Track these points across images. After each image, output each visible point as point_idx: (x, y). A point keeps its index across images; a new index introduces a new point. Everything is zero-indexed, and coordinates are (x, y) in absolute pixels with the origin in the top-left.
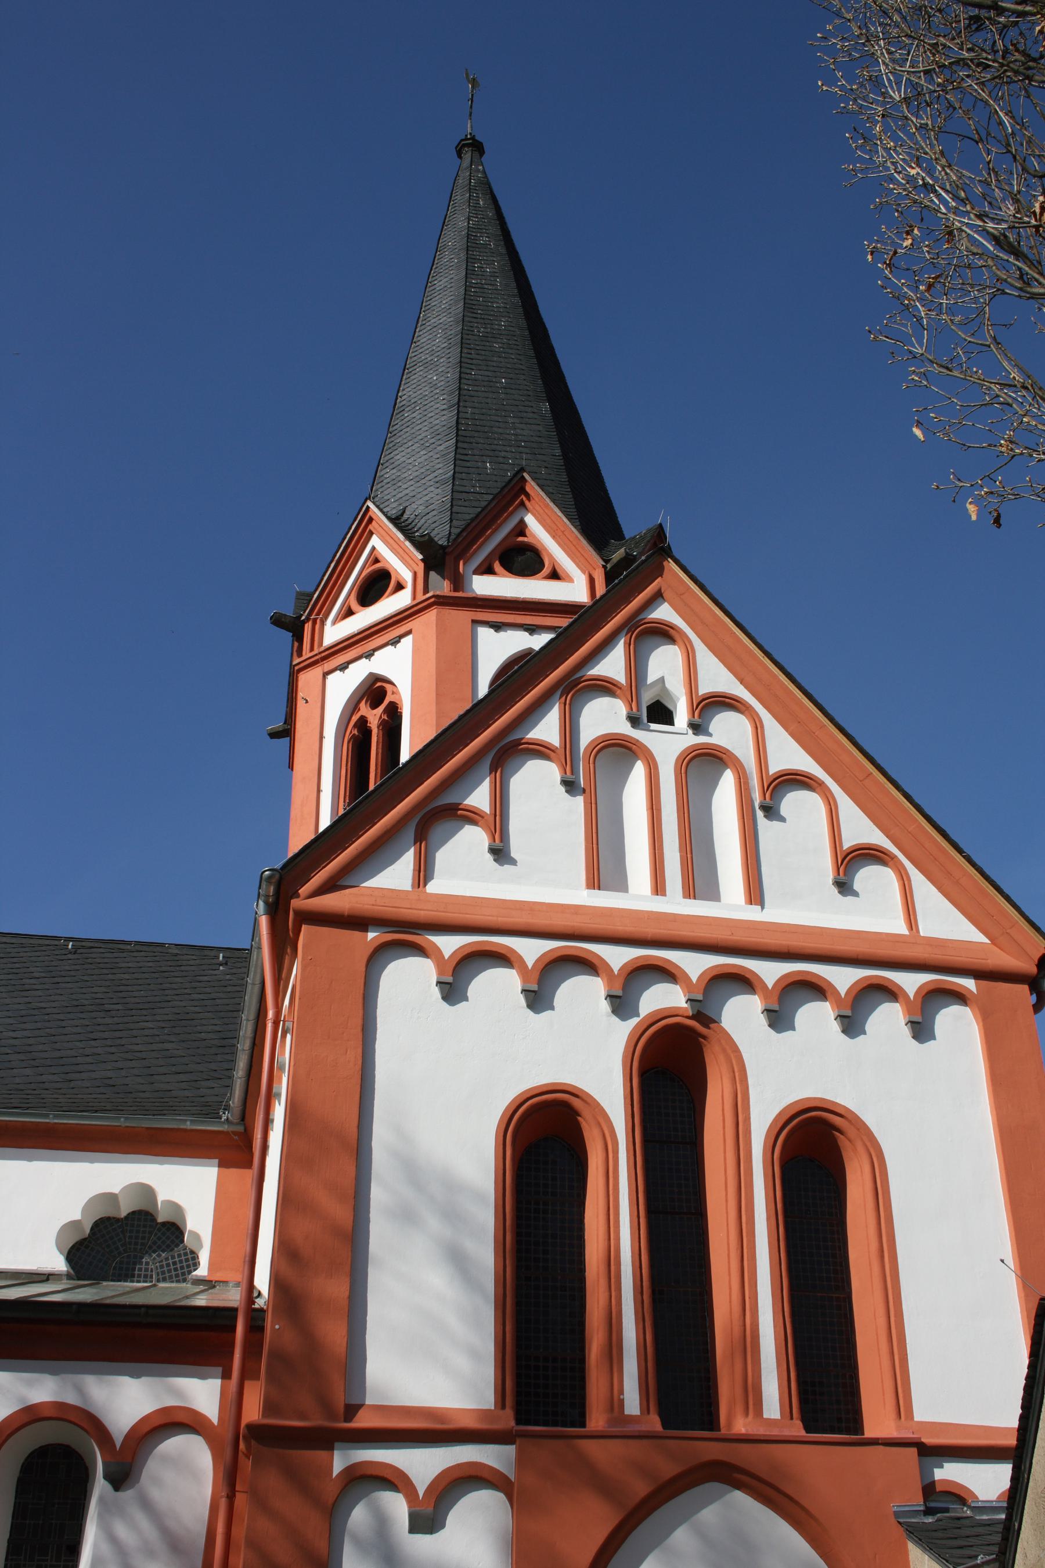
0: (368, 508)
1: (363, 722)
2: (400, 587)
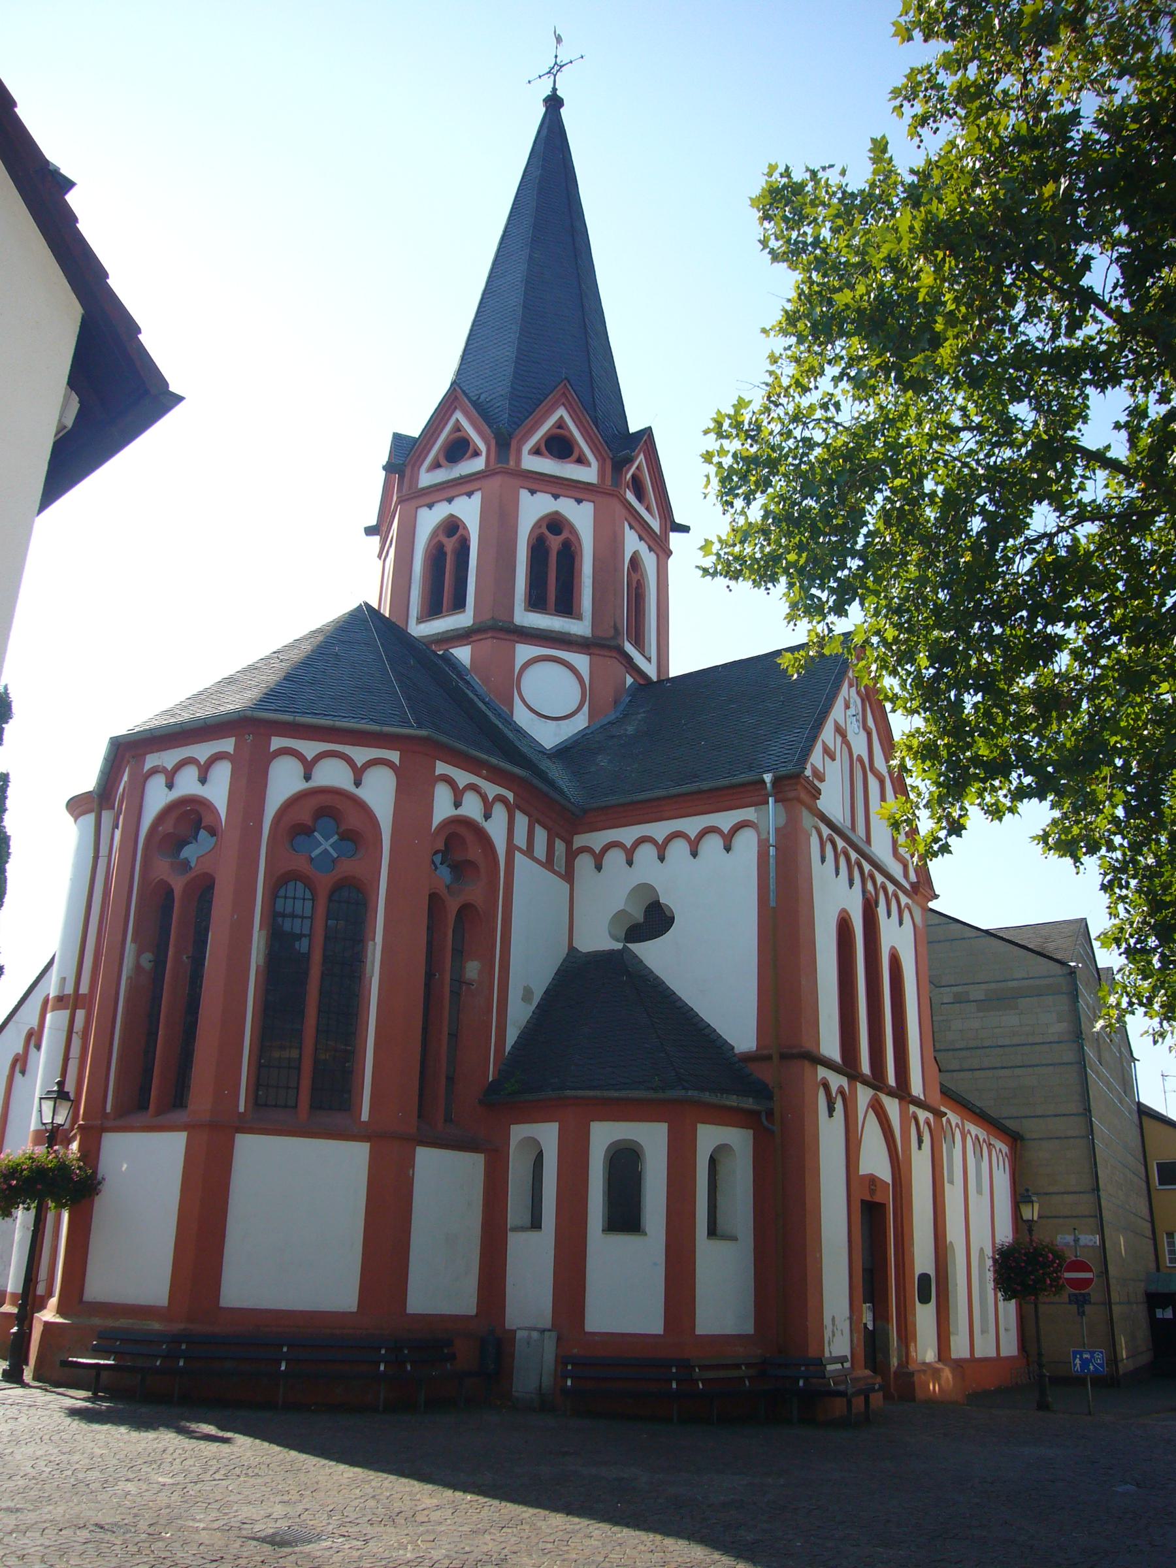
2: (477, 454)
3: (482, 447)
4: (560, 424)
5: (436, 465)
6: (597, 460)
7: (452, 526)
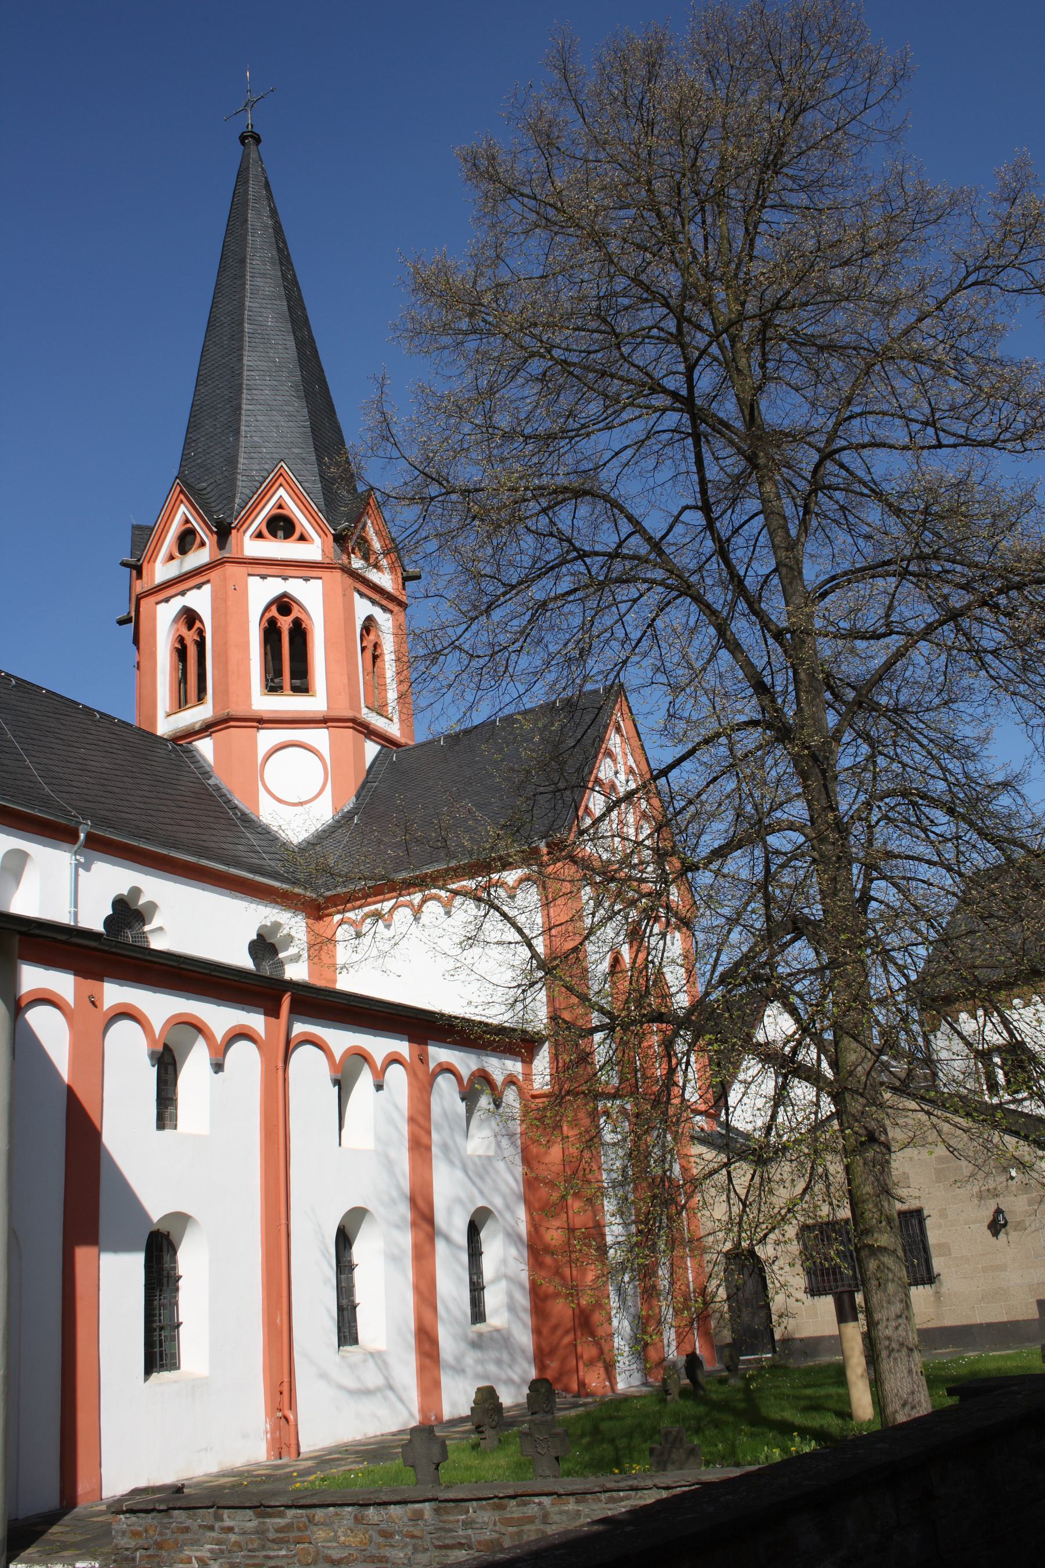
2: (203, 544)
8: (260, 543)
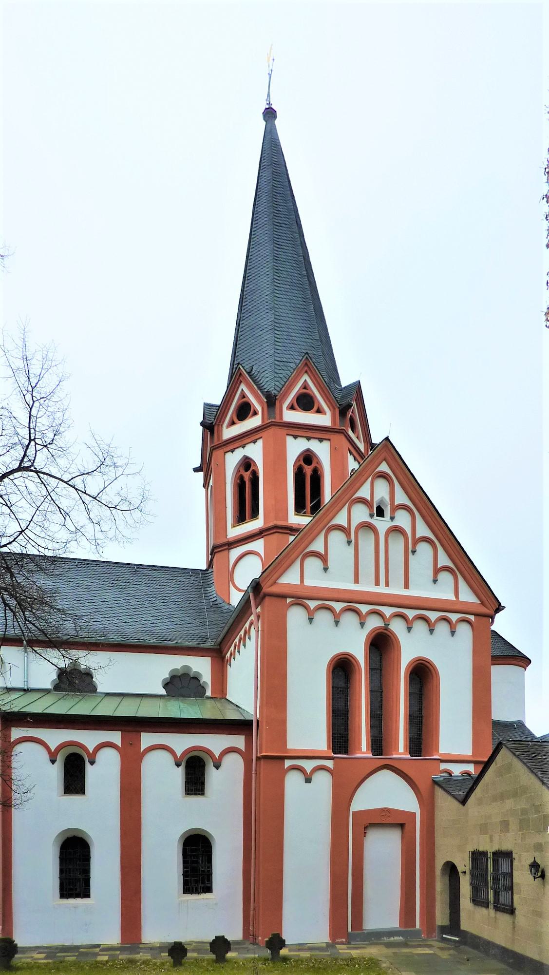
0: (239, 368)
1: (241, 478)
2: (255, 413)
3: (259, 408)
4: (305, 386)
5: (233, 423)
6: (330, 410)
7: (247, 463)
8: (292, 412)
